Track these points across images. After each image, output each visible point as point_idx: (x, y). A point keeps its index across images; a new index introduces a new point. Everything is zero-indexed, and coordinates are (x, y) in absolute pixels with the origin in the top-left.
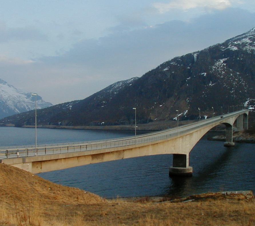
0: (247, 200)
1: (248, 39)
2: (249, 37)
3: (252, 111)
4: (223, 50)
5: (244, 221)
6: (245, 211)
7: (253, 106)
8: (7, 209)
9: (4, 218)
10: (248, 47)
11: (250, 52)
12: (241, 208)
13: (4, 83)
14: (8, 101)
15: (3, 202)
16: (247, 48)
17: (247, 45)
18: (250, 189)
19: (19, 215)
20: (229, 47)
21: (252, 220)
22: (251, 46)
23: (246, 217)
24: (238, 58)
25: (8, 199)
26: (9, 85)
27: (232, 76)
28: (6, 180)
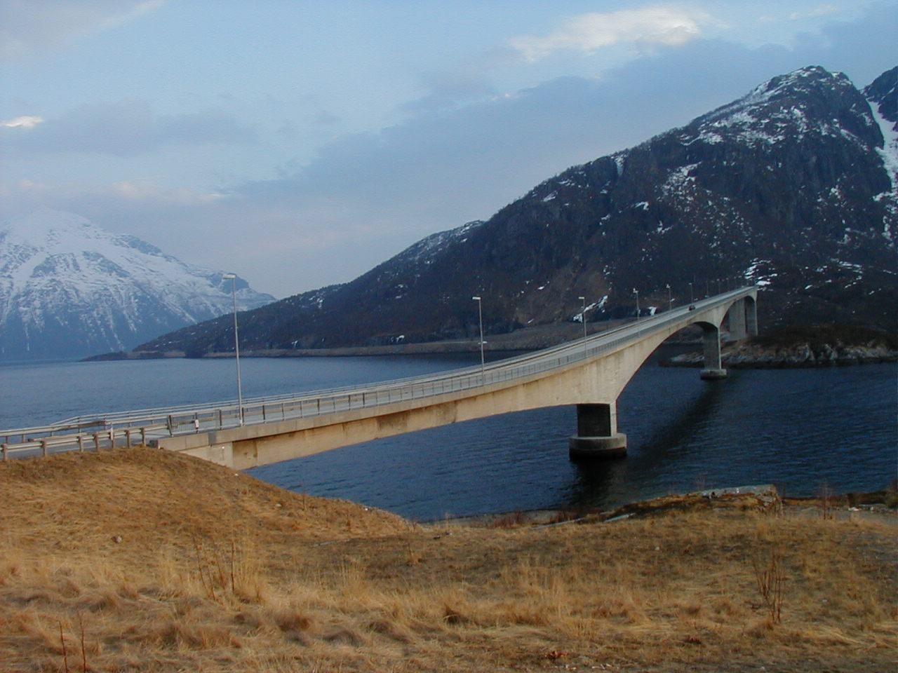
0: (764, 509)
1: (745, 114)
2: (749, 109)
3: (764, 289)
4: (686, 144)
5: (760, 559)
6: (759, 535)
7: (768, 278)
8: (177, 560)
9: (170, 582)
10: (748, 133)
11: (754, 146)
12: (750, 528)
13: (154, 252)
14: (167, 294)
15: (167, 543)
16: (746, 137)
17: (745, 128)
18: (771, 480)
19: (208, 574)
20: (701, 137)
21: (779, 557)
22: (755, 132)
23: (763, 550)
24: (725, 163)
25: (178, 534)
26: (166, 257)
27: (713, 206)
28: (171, 489)
